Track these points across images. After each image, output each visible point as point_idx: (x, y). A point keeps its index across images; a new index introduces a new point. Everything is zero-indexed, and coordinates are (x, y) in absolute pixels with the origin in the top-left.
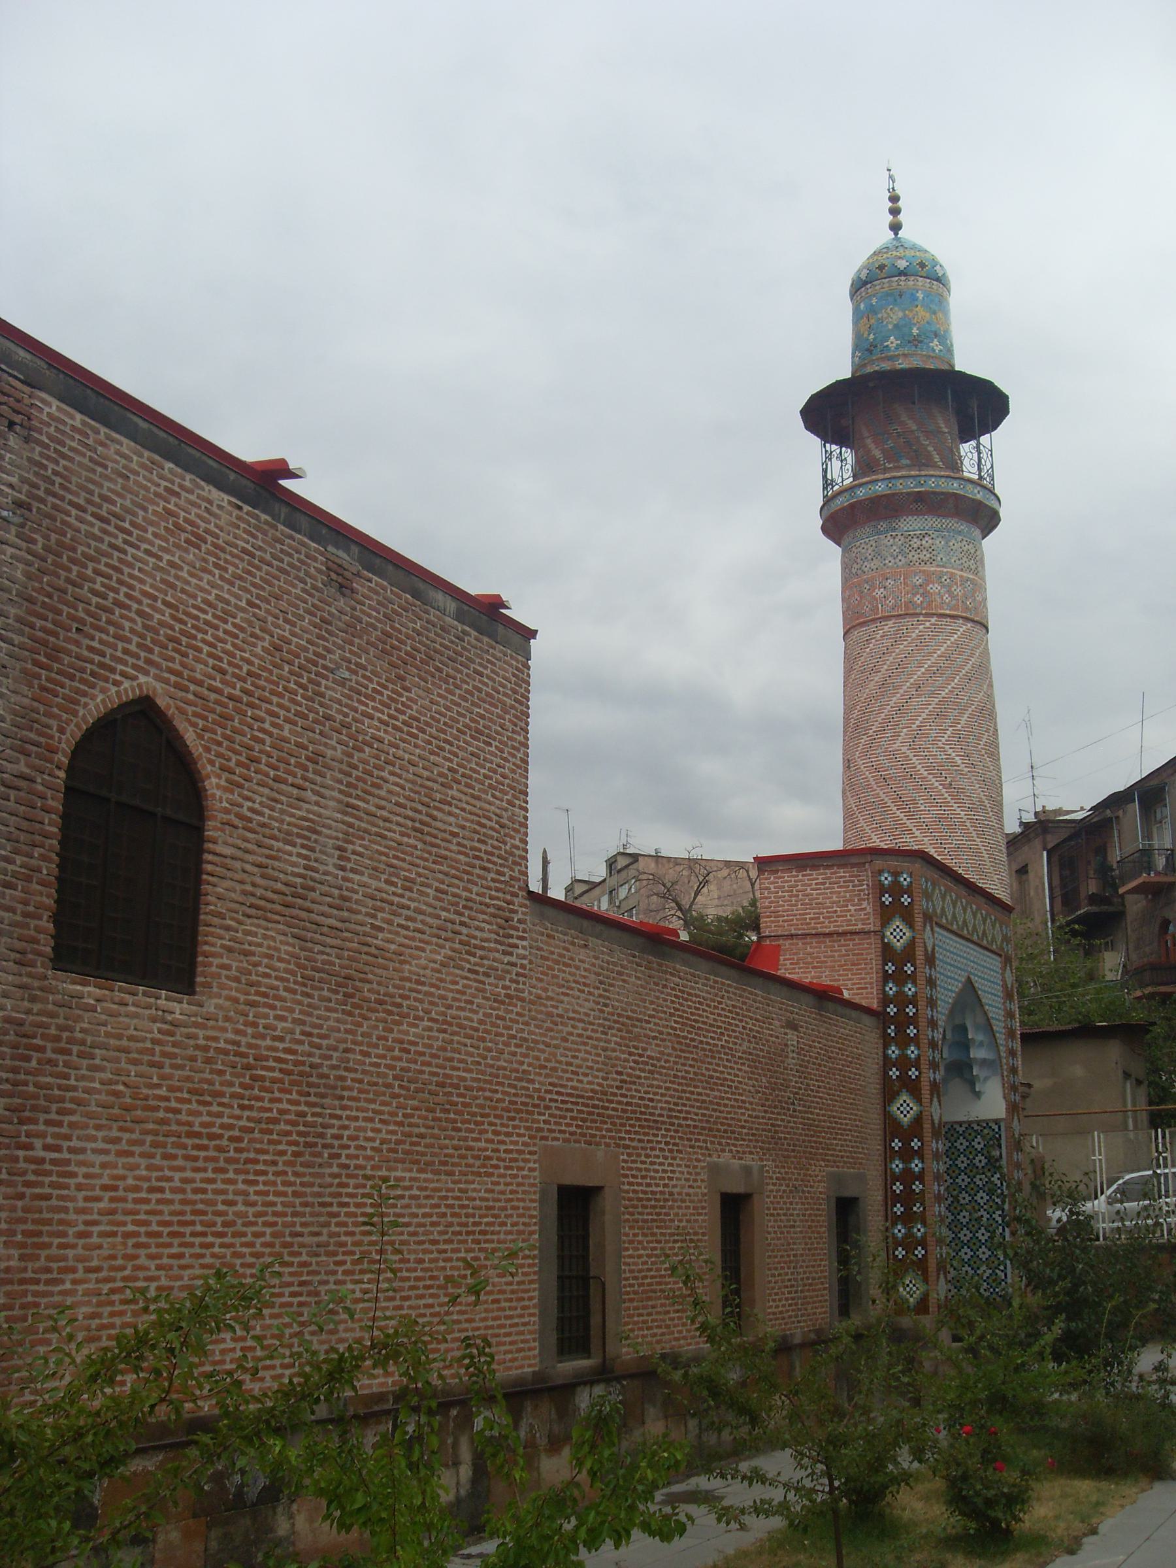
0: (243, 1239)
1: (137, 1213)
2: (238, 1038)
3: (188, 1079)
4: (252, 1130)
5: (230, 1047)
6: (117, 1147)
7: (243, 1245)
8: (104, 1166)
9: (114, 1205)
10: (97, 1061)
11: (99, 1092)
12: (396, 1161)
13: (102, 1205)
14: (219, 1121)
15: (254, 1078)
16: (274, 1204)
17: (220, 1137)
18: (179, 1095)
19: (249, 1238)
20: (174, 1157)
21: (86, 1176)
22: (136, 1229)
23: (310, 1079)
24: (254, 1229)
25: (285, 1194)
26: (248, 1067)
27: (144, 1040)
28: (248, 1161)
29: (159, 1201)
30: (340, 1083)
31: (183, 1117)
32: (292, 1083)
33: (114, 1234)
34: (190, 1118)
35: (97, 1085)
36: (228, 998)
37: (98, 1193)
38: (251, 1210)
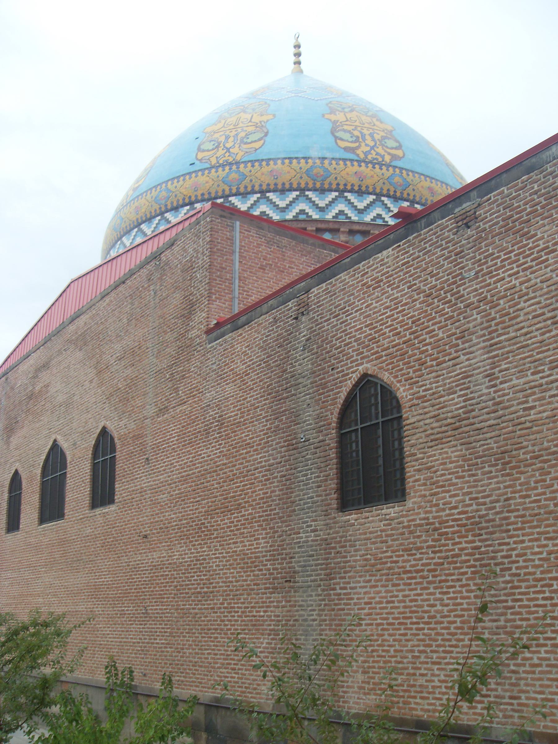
0: (442, 625)
1: (382, 614)
2: (427, 515)
3: (401, 544)
4: (443, 564)
5: (423, 522)
6: (370, 584)
7: (442, 628)
8: (365, 593)
9: (370, 611)
10: (358, 547)
11: (359, 560)
13: (366, 611)
14: (421, 562)
15: (440, 534)
16: (462, 604)
17: (422, 571)
18: (397, 553)
19: (445, 625)
20: (399, 585)
21: (358, 599)
22: (382, 621)
23: (480, 525)
24: (449, 619)
25: (469, 598)
26: (435, 529)
27: (377, 532)
28: (440, 582)
29: (392, 608)
30: (504, 522)
31: (400, 564)
32: (467, 531)
33: (371, 624)
34: (404, 564)
35: (358, 558)
36: (420, 496)
37: (363, 606)
38: (446, 609)
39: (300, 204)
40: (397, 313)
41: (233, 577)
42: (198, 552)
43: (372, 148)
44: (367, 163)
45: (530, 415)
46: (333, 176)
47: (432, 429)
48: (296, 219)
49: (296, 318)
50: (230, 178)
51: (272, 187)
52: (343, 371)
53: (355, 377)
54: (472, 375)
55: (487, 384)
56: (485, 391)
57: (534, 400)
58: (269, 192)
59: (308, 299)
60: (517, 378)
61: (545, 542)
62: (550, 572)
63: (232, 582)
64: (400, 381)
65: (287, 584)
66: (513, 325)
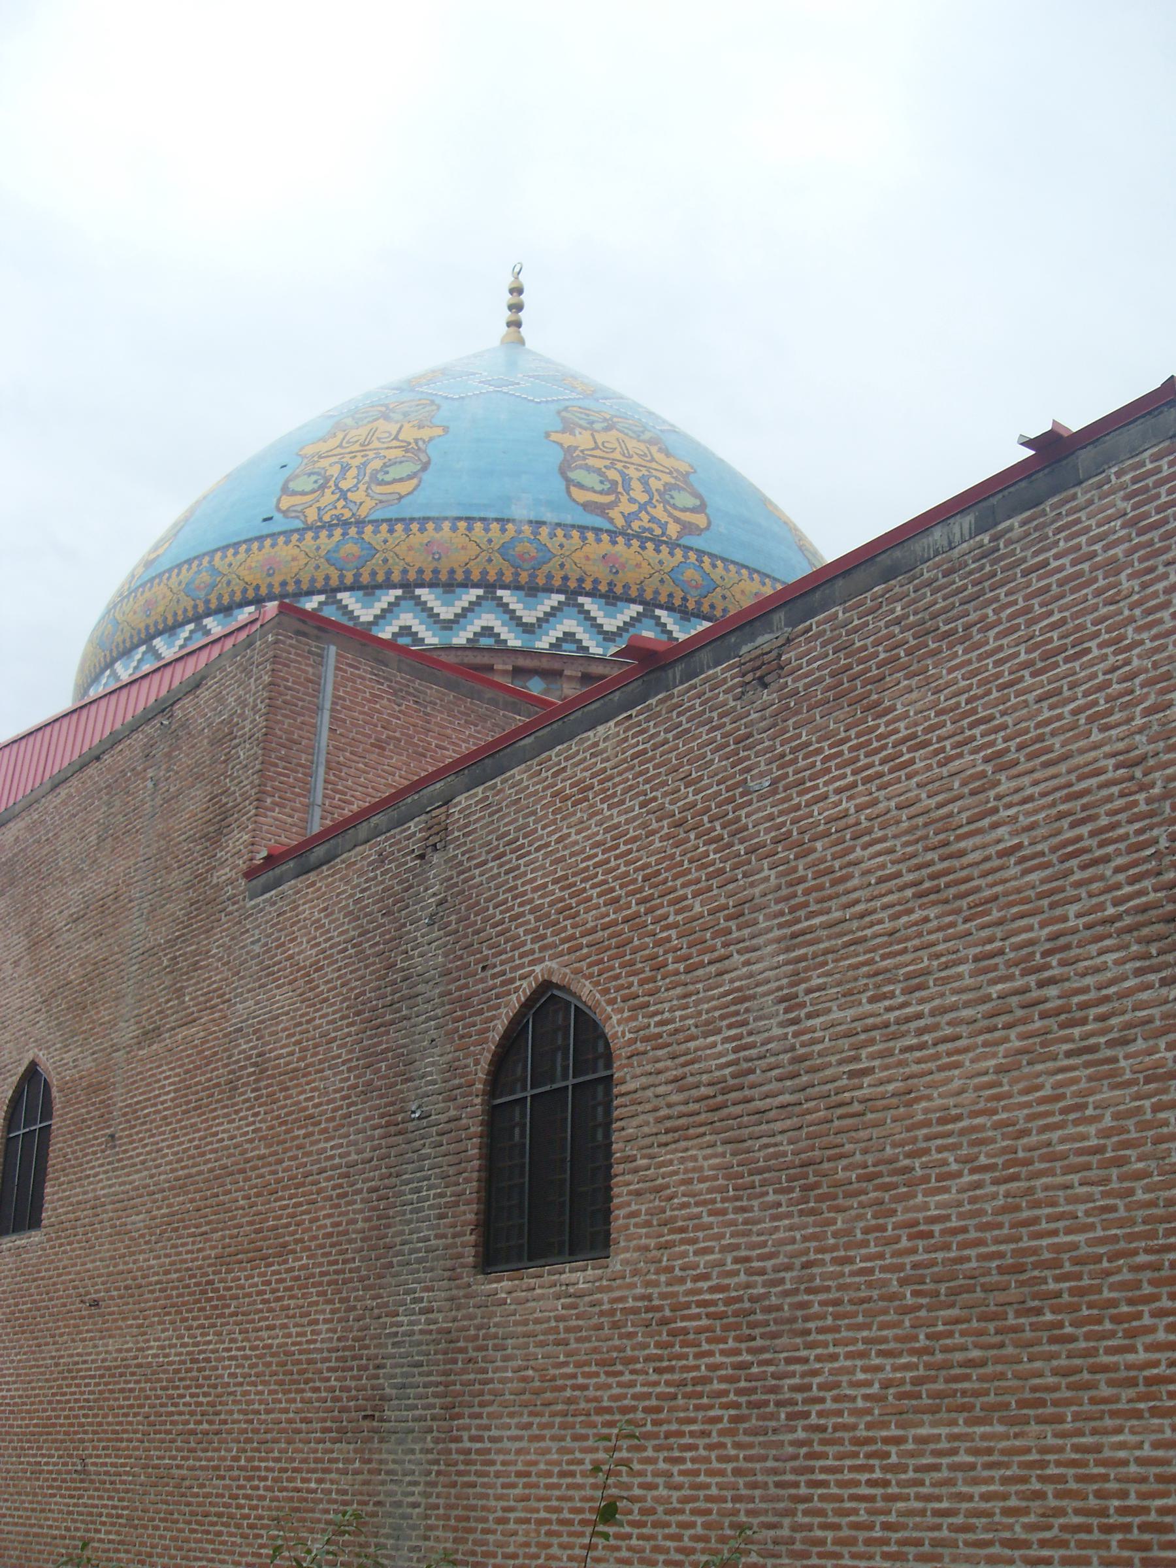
0: (667, 1531)
1: (549, 1499)
2: (650, 1290)
3: (595, 1350)
4: (674, 1397)
5: (640, 1304)
6: (529, 1432)
7: (667, 1537)
8: (519, 1452)
9: (527, 1491)
10: (509, 1351)
11: (511, 1380)
12: (917, 1410)
13: (517, 1491)
14: (631, 1391)
15: (673, 1333)
16: (707, 1486)
17: (634, 1409)
18: (587, 1369)
19: (673, 1530)
20: (585, 1438)
21: (504, 1463)
22: (547, 1515)
23: (752, 1318)
24: (680, 1518)
25: (722, 1473)
26: (664, 1322)
27: (548, 1320)
28: (668, 1435)
29: (569, 1487)
30: (799, 1313)
31: (591, 1393)
32: (726, 1328)
33: (527, 1521)
34: (599, 1393)
35: (510, 1374)
36: (639, 1249)
37: (513, 1479)
38: (676, 1494)
39: (484, 616)
40: (617, 858)
41: (261, 1402)
42: (196, 1344)
43: (643, 507)
44: (628, 538)
45: (861, 1087)
46: (556, 562)
47: (669, 1106)
48: (472, 647)
49: (422, 857)
50: (342, 553)
51: (428, 576)
52: (504, 973)
53: (526, 987)
54: (753, 997)
55: (781, 1017)
56: (777, 1031)
57: (872, 1057)
58: (422, 586)
59: (448, 816)
60: (841, 1008)
61: (877, 1361)
62: (885, 1425)
63: (258, 1412)
64: (611, 1002)
65: (365, 1424)
66: (838, 896)
